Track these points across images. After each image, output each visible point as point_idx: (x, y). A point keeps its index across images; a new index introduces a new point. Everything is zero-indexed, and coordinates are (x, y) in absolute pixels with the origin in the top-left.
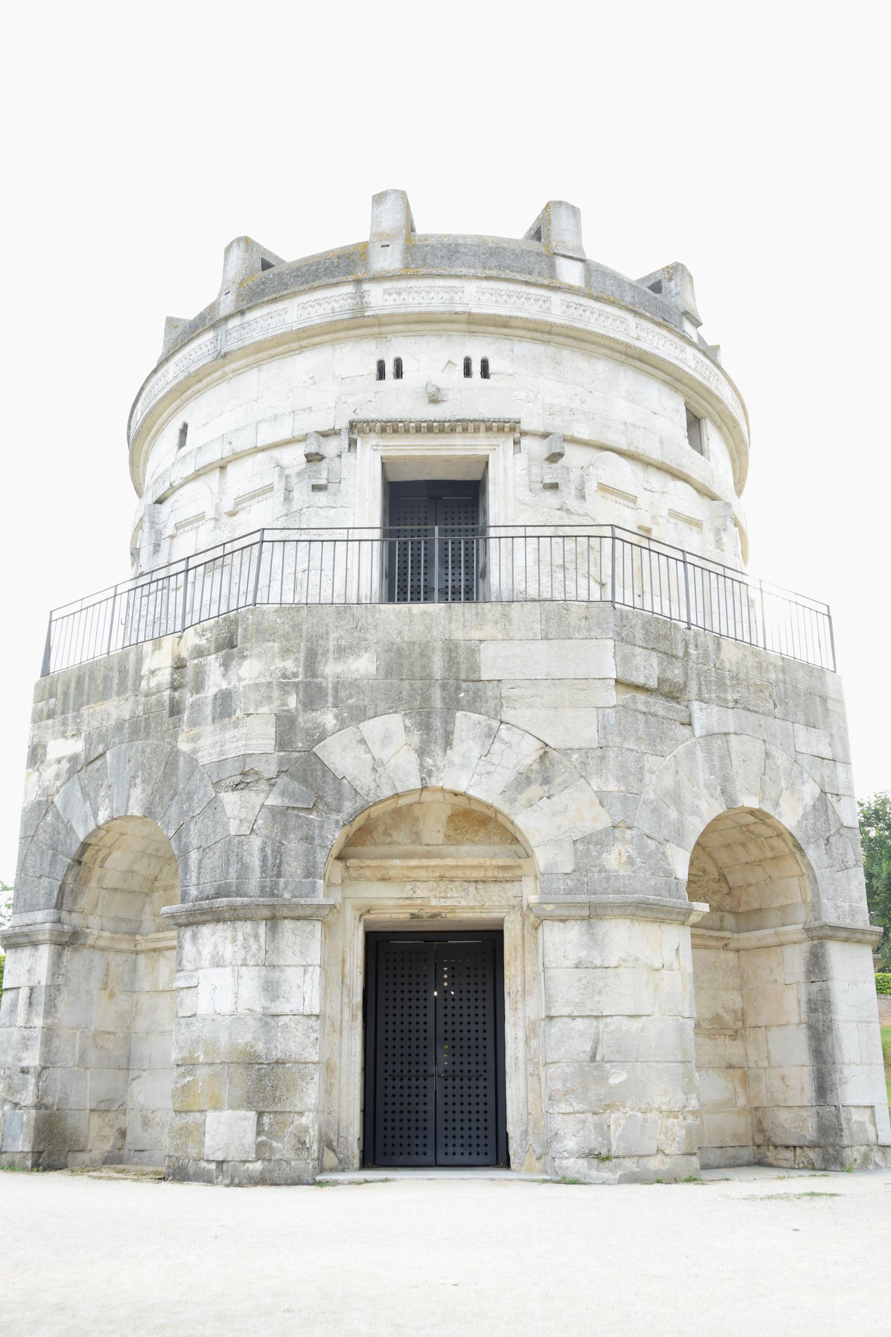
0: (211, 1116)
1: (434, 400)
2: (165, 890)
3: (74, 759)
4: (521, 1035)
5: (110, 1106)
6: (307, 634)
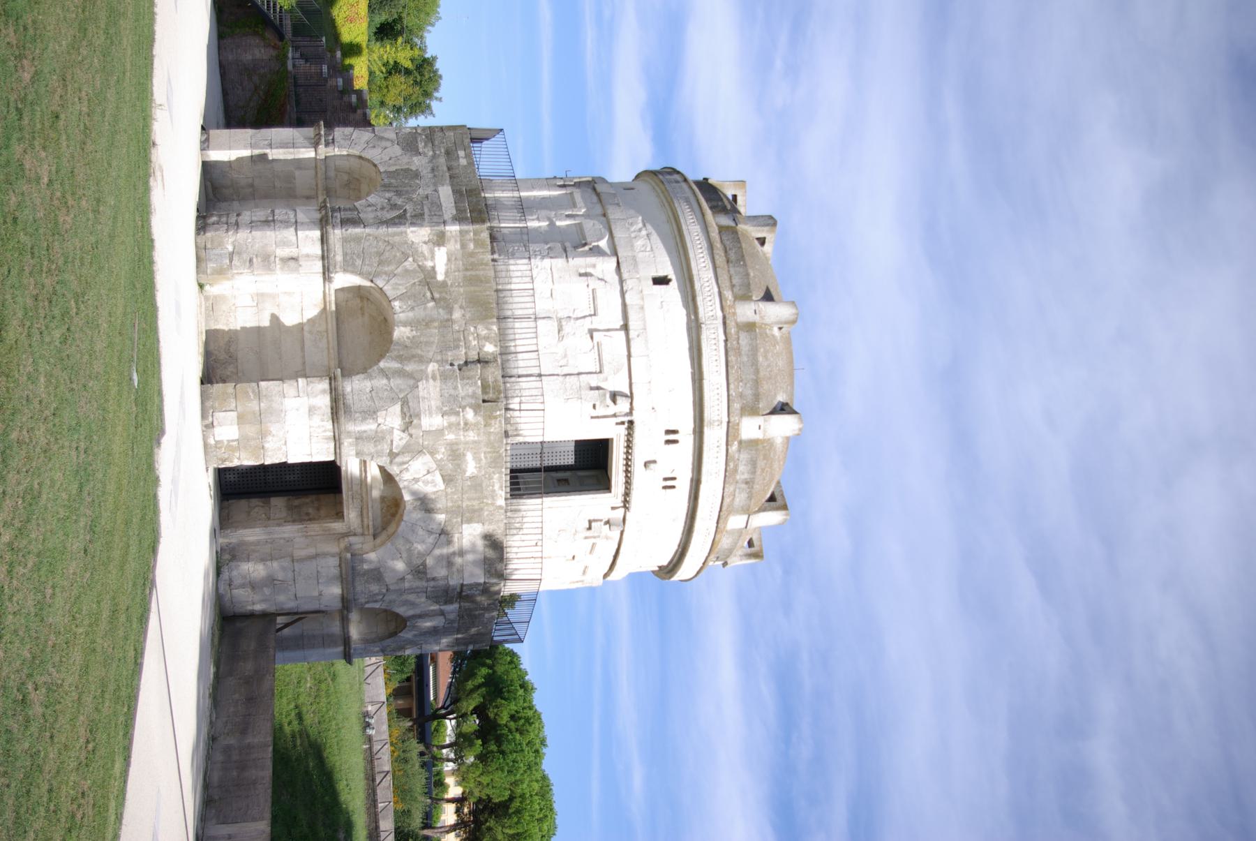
0: (234, 414)
2: (362, 309)
4: (286, 535)
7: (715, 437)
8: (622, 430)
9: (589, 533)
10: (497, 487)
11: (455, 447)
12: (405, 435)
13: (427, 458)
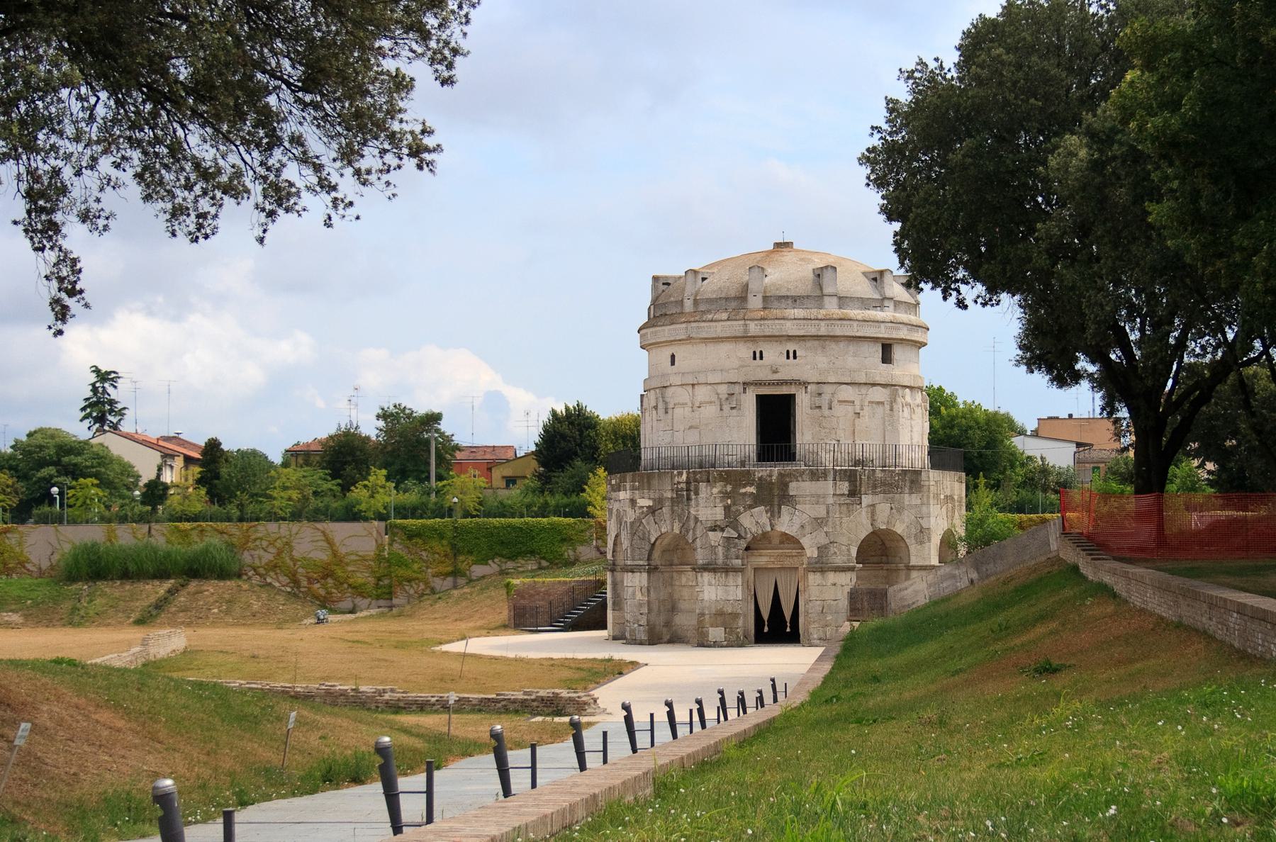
1: (775, 372)
3: (649, 507)
5: (668, 624)
6: (734, 478)
7: (754, 328)
9: (825, 407)
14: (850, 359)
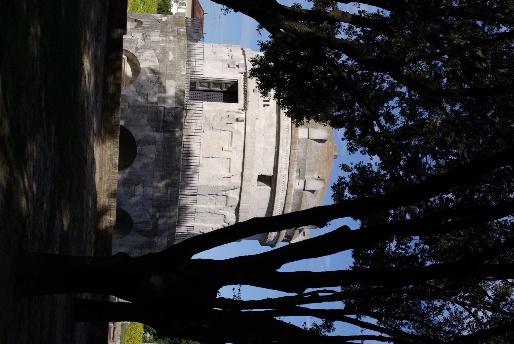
8: (242, 76)
10: (182, 66)
11: (164, 49)
12: (143, 42)
13: (152, 51)
14: (262, 146)
